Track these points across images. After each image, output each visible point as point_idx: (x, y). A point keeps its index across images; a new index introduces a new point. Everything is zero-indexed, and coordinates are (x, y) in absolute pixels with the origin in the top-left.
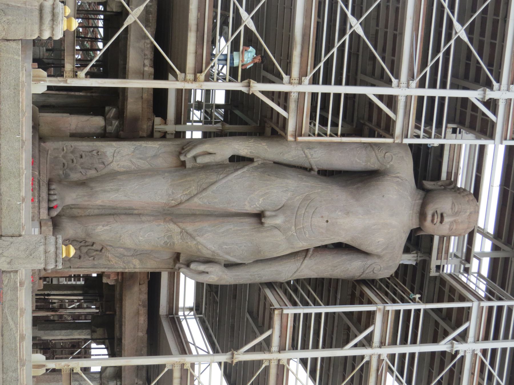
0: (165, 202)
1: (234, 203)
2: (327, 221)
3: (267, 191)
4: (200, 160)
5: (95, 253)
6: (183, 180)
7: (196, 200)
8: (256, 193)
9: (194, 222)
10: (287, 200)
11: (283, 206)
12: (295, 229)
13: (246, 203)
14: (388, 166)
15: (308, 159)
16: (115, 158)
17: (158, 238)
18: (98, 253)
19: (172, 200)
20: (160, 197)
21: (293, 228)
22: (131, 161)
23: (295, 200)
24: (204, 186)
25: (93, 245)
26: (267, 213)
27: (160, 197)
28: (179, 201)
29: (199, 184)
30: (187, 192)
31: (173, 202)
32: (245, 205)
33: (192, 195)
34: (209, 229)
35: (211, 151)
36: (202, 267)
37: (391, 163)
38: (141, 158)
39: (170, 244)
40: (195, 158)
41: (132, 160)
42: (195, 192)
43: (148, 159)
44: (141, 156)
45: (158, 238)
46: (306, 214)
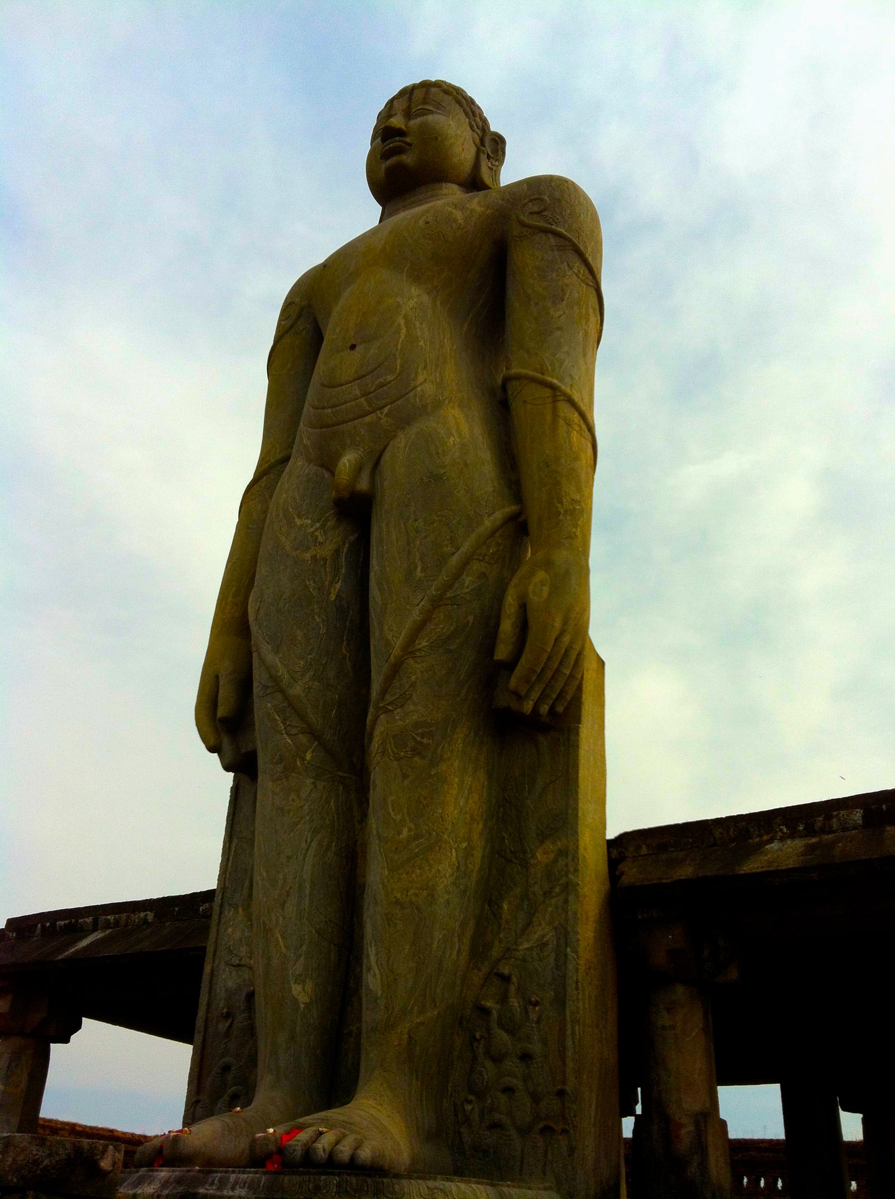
0: (309, 781)
1: (306, 587)
5: (515, 1003)
7: (297, 690)
8: (283, 539)
11: (322, 466)
13: (308, 556)
16: (243, 962)
17: (405, 776)
18: (513, 989)
19: (303, 759)
20: (293, 796)
21: (367, 419)
25: (486, 1012)
27: (293, 796)
28: (303, 739)
31: (308, 756)
32: (314, 558)
36: (507, 626)
39: (423, 735)
45: (405, 776)
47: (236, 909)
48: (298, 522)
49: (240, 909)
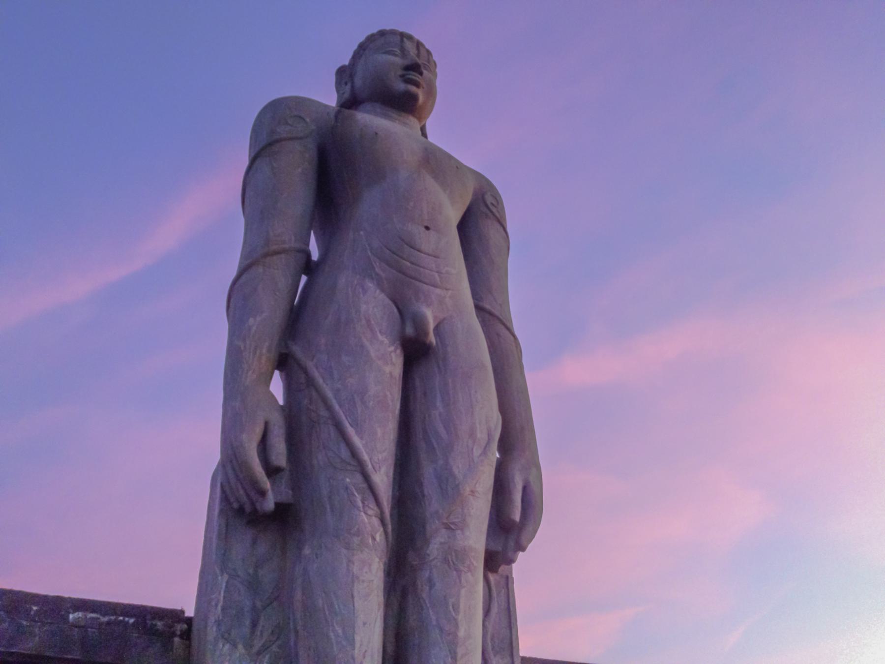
2: (427, 228)
3: (364, 322)
4: (280, 454)
6: (328, 507)
9: (424, 496)
10: (383, 290)
14: (313, 127)
19: (374, 539)
21: (438, 291)
22: (259, 653)
23: (383, 275)
24: (345, 453)
26: (410, 331)
28: (376, 522)
31: (378, 538)
32: (391, 373)
33: (365, 485)
34: (441, 462)
35: (259, 430)
37: (308, 120)
40: (272, 471)
41: (255, 649)
42: (359, 478)
43: (259, 604)
44: (248, 622)
47: (234, 646)
49: (240, 647)
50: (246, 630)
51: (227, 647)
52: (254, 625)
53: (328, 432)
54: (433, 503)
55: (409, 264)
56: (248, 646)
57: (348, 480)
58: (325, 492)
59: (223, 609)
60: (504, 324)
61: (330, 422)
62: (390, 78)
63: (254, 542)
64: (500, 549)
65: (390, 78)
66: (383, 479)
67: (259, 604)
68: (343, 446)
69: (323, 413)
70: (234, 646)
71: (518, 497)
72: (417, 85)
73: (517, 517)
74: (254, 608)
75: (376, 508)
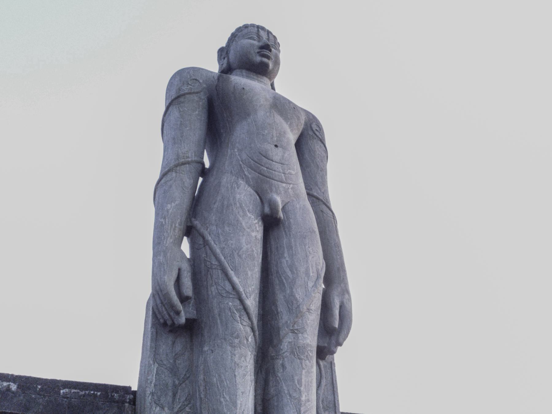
1: (253, 251)
2: (276, 146)
3: (238, 205)
4: (188, 289)
6: (219, 321)
8: (241, 219)
9: (278, 313)
10: (249, 185)
12: (285, 183)
15: (192, 161)
19: (247, 340)
21: (284, 185)
23: (250, 176)
24: (229, 287)
26: (267, 210)
28: (248, 329)
29: (225, 295)
30: (237, 315)
31: (250, 340)
32: (256, 236)
33: (241, 307)
34: (288, 292)
37: (201, 81)
38: (174, 395)
40: (184, 299)
43: (177, 382)
44: (170, 394)
46: (267, 166)
48: (249, 215)
49: (166, 409)
50: (170, 399)
51: (158, 408)
52: (174, 395)
53: (217, 273)
54: (284, 317)
55: (265, 169)
56: (171, 409)
57: (230, 304)
58: (216, 311)
59: (155, 385)
60: (326, 205)
61: (218, 267)
62: (252, 54)
63: (174, 343)
64: (326, 345)
65: (252, 54)
66: (252, 302)
67: (177, 382)
68: (227, 283)
69: (214, 262)
70: (163, 408)
71: (337, 312)
72: (268, 57)
73: (336, 325)
74: (175, 386)
75: (248, 321)
